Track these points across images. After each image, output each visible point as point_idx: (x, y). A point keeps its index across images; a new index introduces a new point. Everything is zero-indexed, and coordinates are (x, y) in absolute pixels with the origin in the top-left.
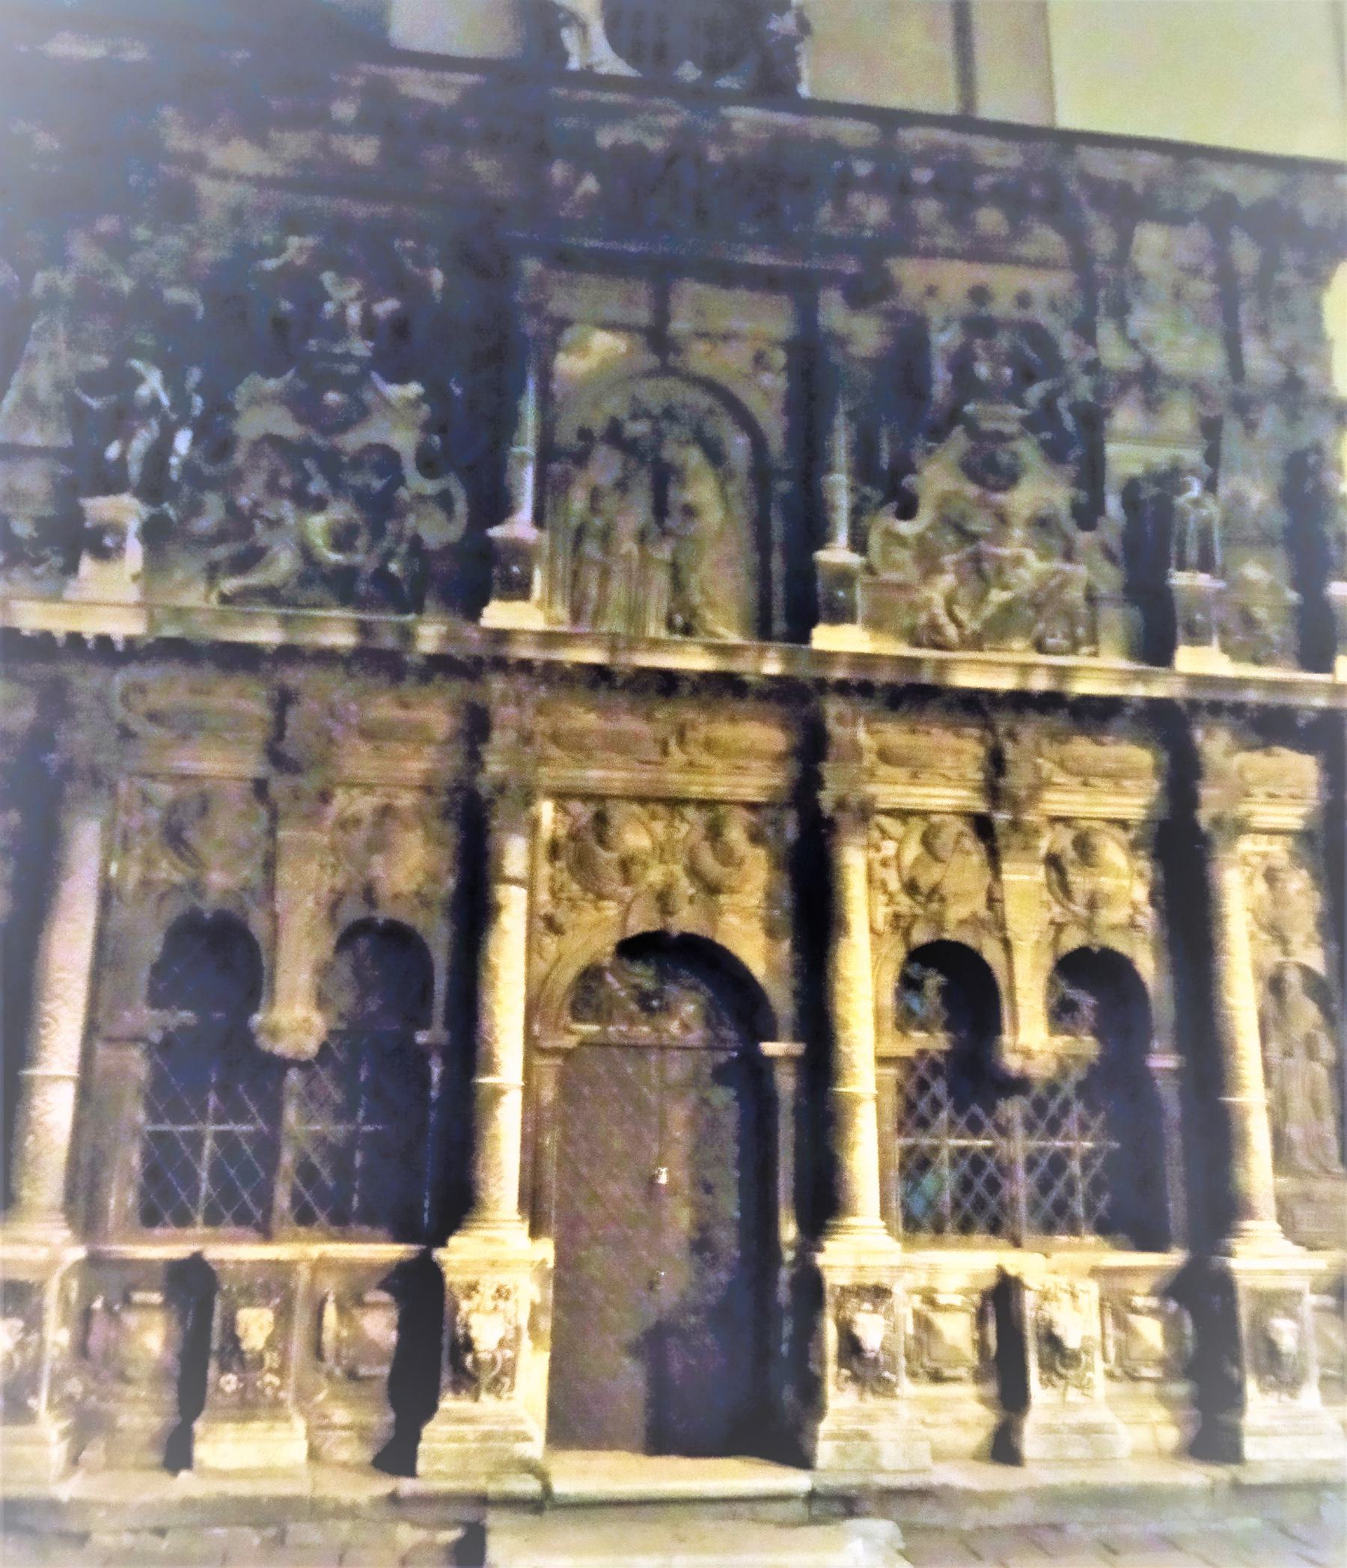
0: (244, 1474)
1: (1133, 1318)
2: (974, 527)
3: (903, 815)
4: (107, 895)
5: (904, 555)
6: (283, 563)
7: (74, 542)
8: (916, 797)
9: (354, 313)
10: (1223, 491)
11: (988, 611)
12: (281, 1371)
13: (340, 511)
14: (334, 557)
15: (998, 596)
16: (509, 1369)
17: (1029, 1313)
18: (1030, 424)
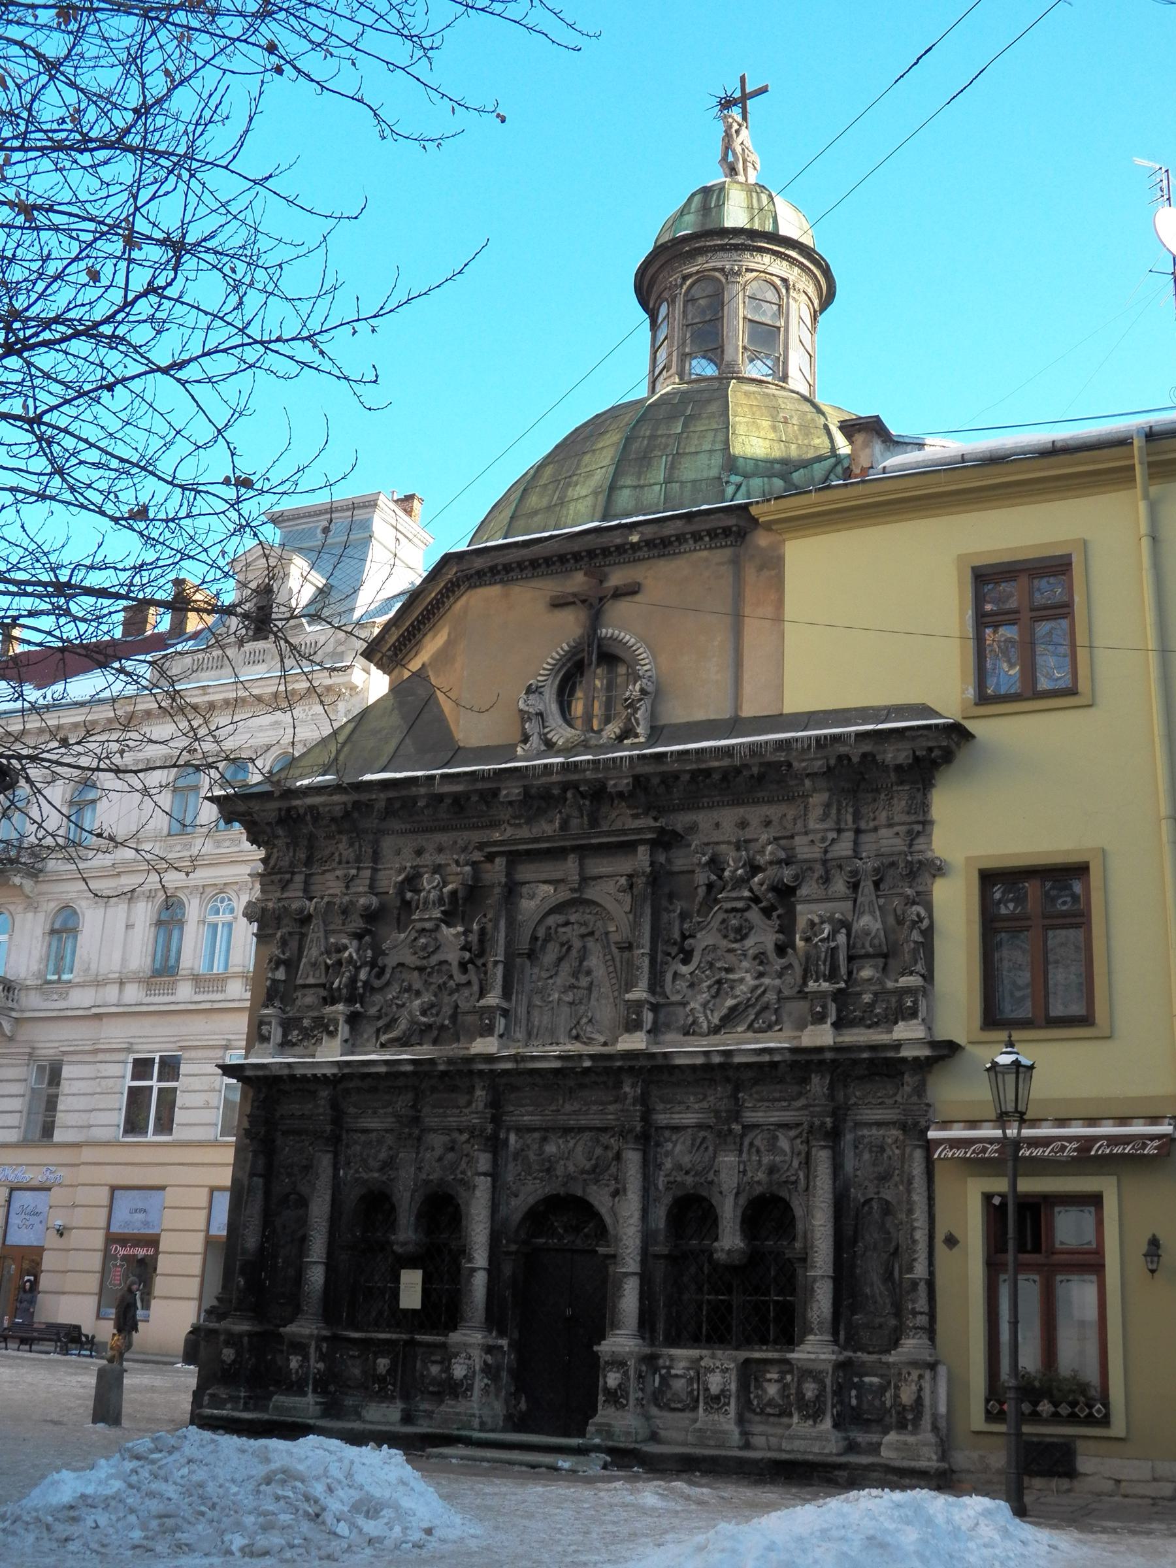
0: (378, 1423)
1: (766, 1384)
2: (718, 965)
3: (676, 1129)
4: (337, 1187)
5: (681, 985)
6: (403, 1025)
7: (325, 1027)
8: (678, 1119)
9: (433, 895)
10: (855, 927)
11: (724, 1011)
12: (394, 1385)
13: (427, 998)
14: (424, 1019)
15: (730, 1002)
16: (470, 1388)
17: (702, 1379)
18: (756, 900)
